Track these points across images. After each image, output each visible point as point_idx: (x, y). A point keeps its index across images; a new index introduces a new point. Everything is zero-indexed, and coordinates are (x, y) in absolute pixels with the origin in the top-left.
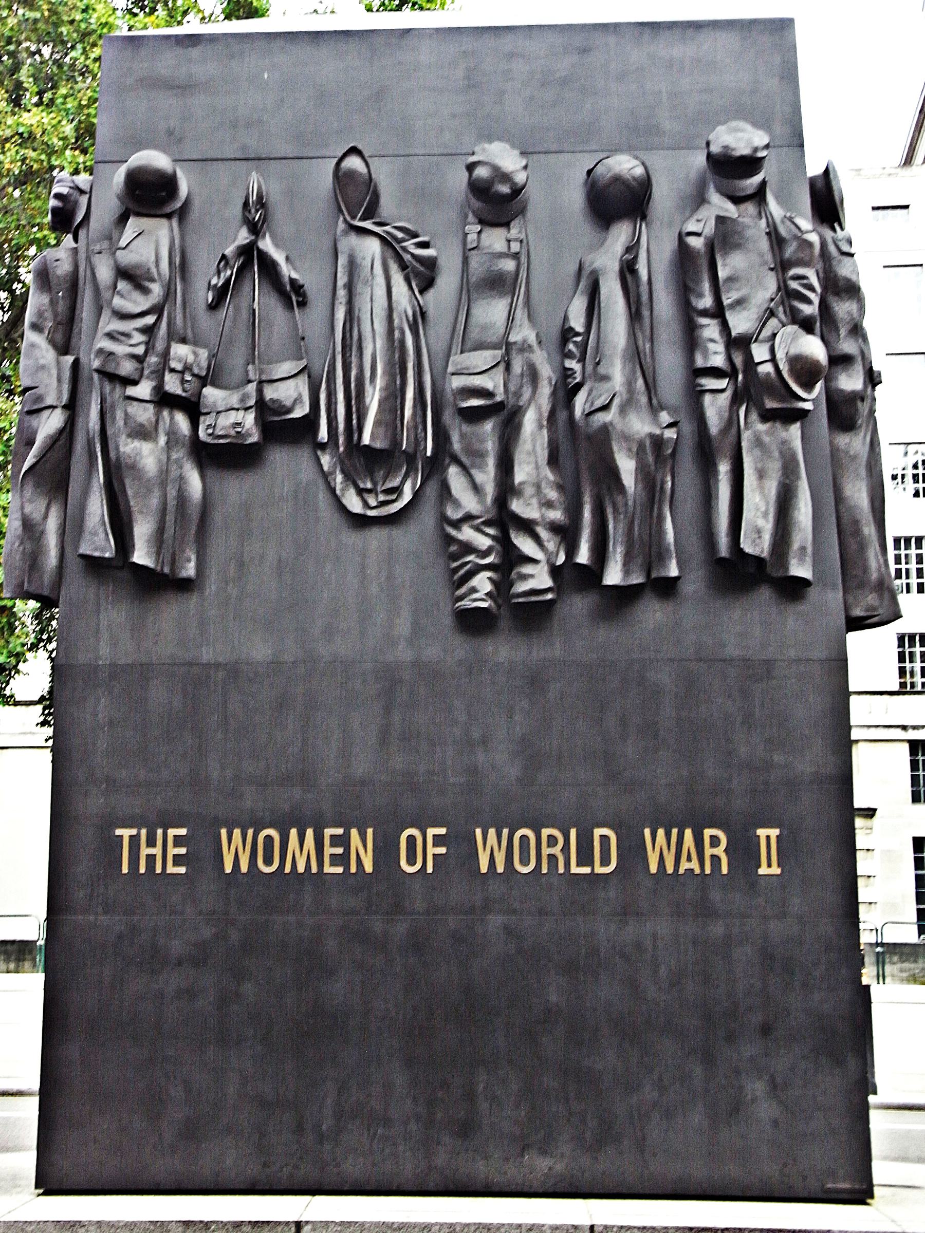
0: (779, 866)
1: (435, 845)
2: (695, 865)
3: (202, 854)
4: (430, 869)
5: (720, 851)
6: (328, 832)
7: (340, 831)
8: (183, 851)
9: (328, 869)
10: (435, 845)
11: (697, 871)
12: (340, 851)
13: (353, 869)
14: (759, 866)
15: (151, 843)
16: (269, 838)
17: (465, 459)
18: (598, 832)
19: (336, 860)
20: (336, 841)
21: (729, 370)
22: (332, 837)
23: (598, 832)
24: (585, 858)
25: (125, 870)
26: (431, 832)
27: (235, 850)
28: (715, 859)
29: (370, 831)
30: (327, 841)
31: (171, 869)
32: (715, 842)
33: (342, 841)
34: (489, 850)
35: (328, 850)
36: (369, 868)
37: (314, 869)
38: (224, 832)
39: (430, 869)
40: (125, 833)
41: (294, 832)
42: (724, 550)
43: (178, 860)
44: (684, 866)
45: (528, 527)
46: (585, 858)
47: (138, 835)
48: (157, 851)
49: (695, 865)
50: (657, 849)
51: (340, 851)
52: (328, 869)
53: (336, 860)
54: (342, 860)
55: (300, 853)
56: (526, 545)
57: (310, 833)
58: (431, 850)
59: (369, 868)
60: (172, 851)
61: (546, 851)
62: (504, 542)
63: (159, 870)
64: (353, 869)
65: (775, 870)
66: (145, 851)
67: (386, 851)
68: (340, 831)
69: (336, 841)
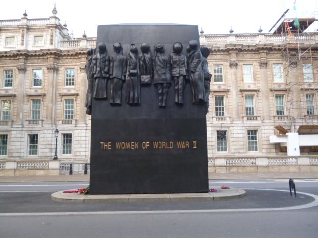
3: (114, 145)
18: (171, 142)
19: (133, 147)
23: (171, 142)
27: (118, 145)
34: (155, 145)
40: (102, 143)
43: (110, 147)
46: (169, 146)
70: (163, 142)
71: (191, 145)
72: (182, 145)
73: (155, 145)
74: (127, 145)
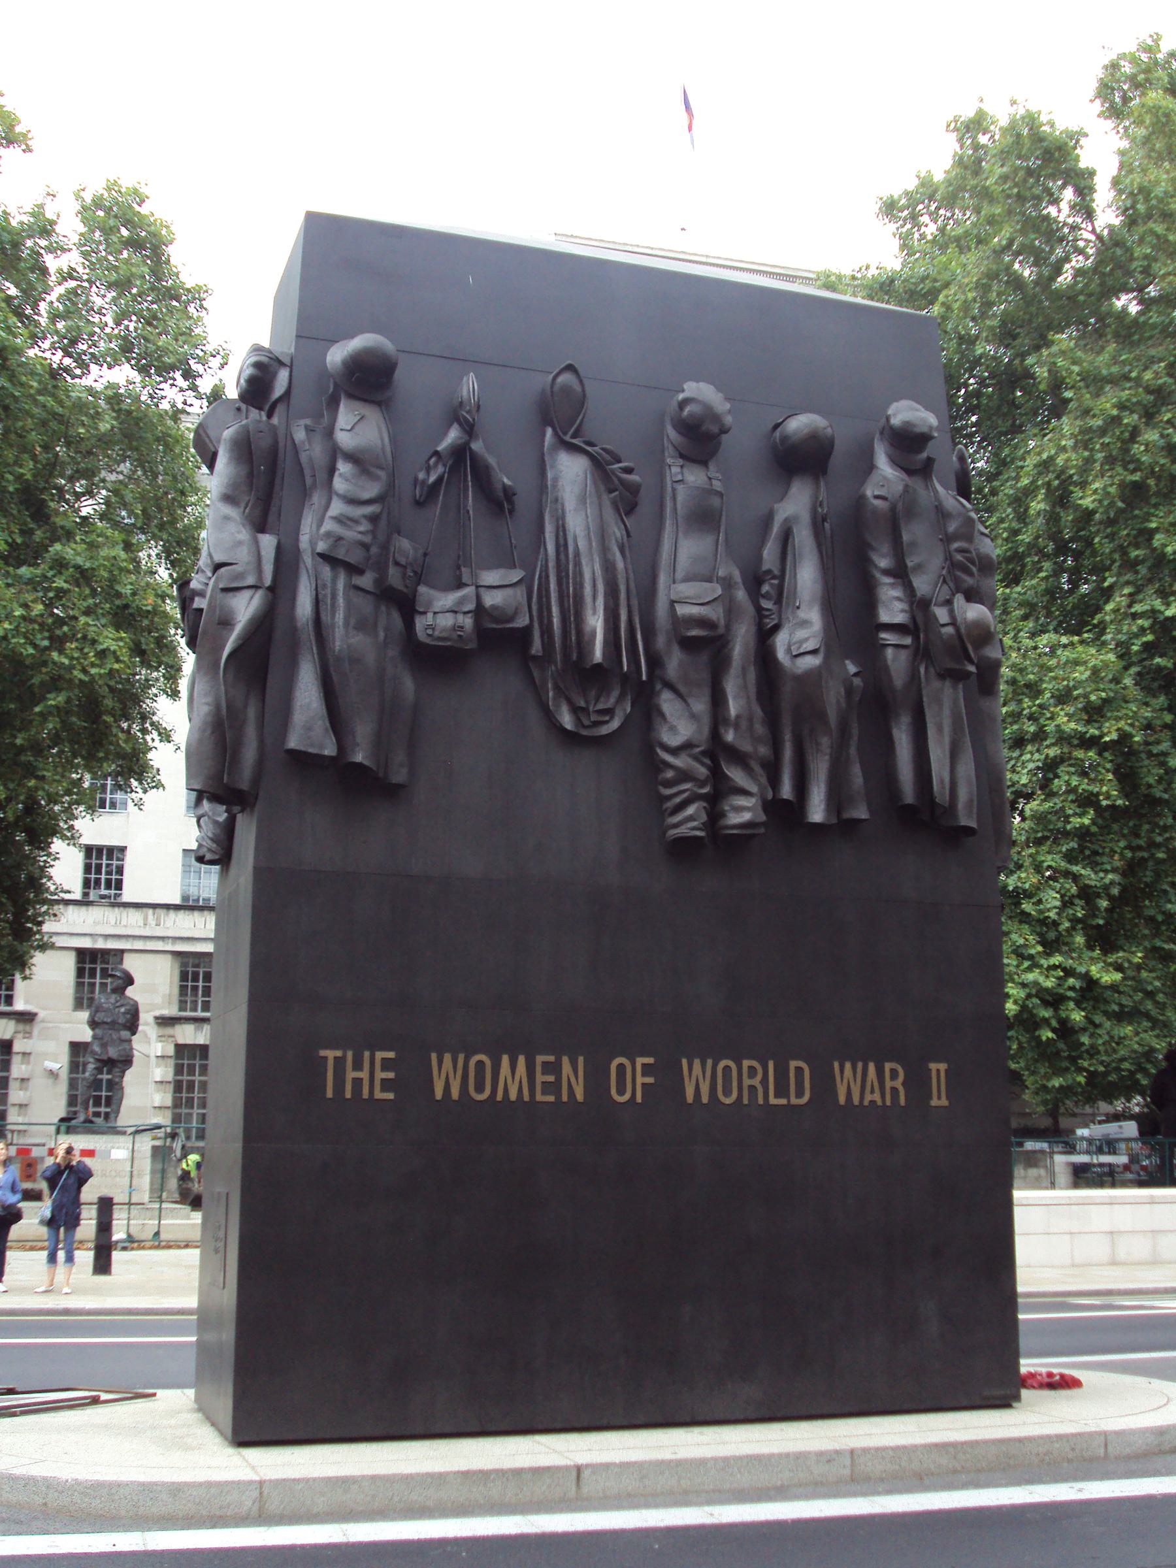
0: (948, 1098)
1: (643, 1075)
2: (877, 1097)
3: (412, 1080)
4: (639, 1099)
5: (898, 1083)
6: (540, 1059)
7: (551, 1058)
8: (391, 1075)
9: (539, 1097)
10: (643, 1075)
11: (879, 1103)
12: (551, 1078)
13: (565, 1098)
14: (930, 1097)
15: (358, 1066)
16: (480, 1064)
17: (682, 689)
18: (793, 1064)
19: (547, 1088)
20: (548, 1068)
21: (911, 626)
22: (544, 1063)
24: (781, 1091)
25: (330, 1094)
26: (640, 1061)
27: (447, 1076)
28: (894, 1090)
29: (581, 1059)
30: (539, 1068)
31: (379, 1095)
32: (894, 1074)
33: (553, 1068)
34: (697, 1080)
35: (540, 1078)
36: (580, 1097)
37: (526, 1098)
38: (434, 1056)
39: (639, 1099)
41: (505, 1059)
42: (909, 793)
43: (386, 1085)
44: (868, 1098)
45: (739, 758)
47: (344, 1057)
48: (364, 1075)
49: (877, 1097)
50: (845, 1081)
51: (551, 1078)
52: (539, 1097)
53: (547, 1088)
54: (553, 1088)
55: (512, 1079)
56: (737, 776)
57: (521, 1059)
58: (640, 1080)
59: (580, 1097)
60: (380, 1075)
61: (747, 1082)
62: (717, 774)
63: (366, 1094)
64: (565, 1098)
65: (944, 1102)
66: (351, 1075)
67: (596, 1079)
68: (551, 1058)
69: (548, 1068)
70: (746, 1063)
71: (918, 1083)
72: (855, 1083)
73: (697, 1080)
74: (512, 1079)
